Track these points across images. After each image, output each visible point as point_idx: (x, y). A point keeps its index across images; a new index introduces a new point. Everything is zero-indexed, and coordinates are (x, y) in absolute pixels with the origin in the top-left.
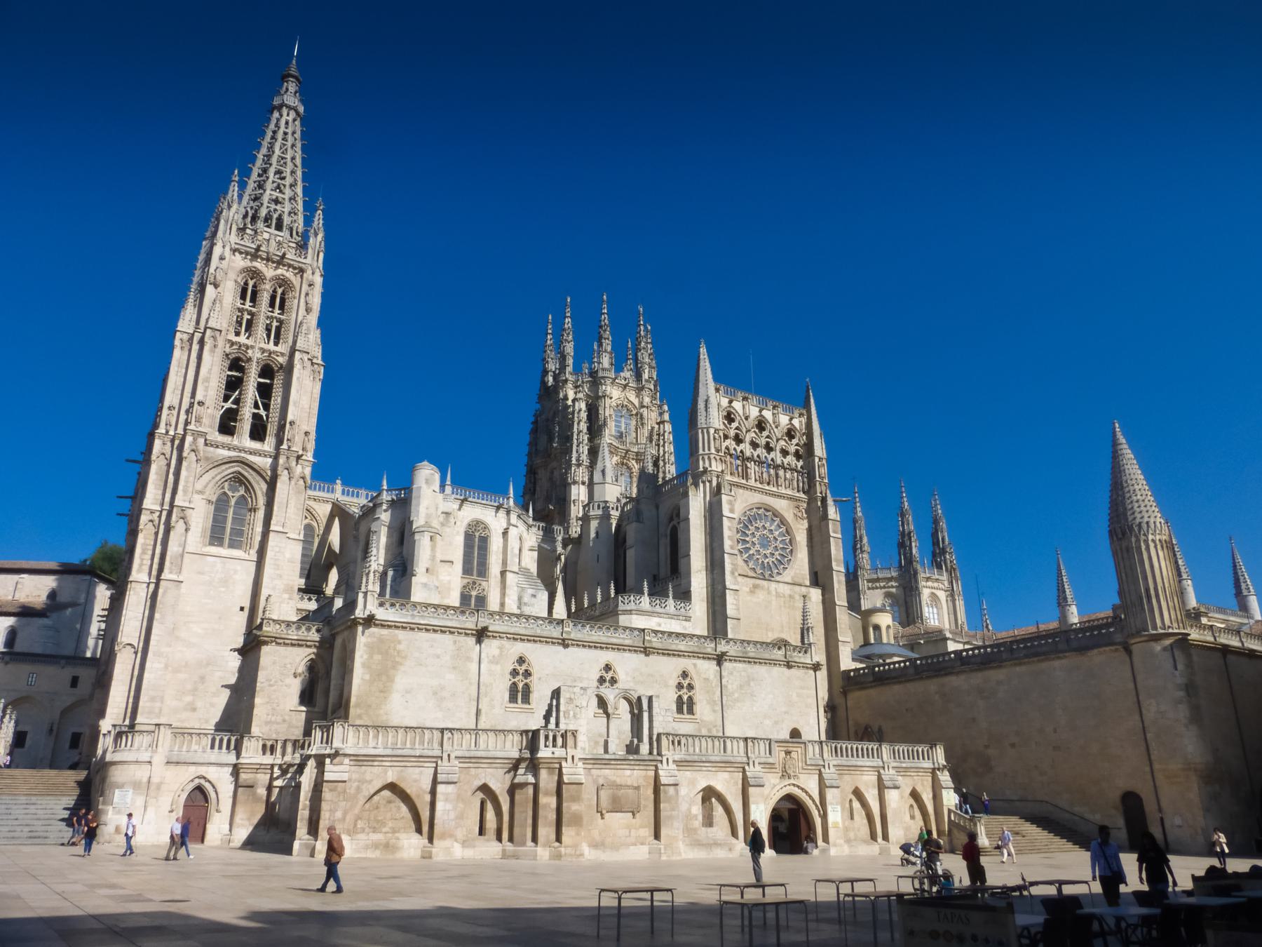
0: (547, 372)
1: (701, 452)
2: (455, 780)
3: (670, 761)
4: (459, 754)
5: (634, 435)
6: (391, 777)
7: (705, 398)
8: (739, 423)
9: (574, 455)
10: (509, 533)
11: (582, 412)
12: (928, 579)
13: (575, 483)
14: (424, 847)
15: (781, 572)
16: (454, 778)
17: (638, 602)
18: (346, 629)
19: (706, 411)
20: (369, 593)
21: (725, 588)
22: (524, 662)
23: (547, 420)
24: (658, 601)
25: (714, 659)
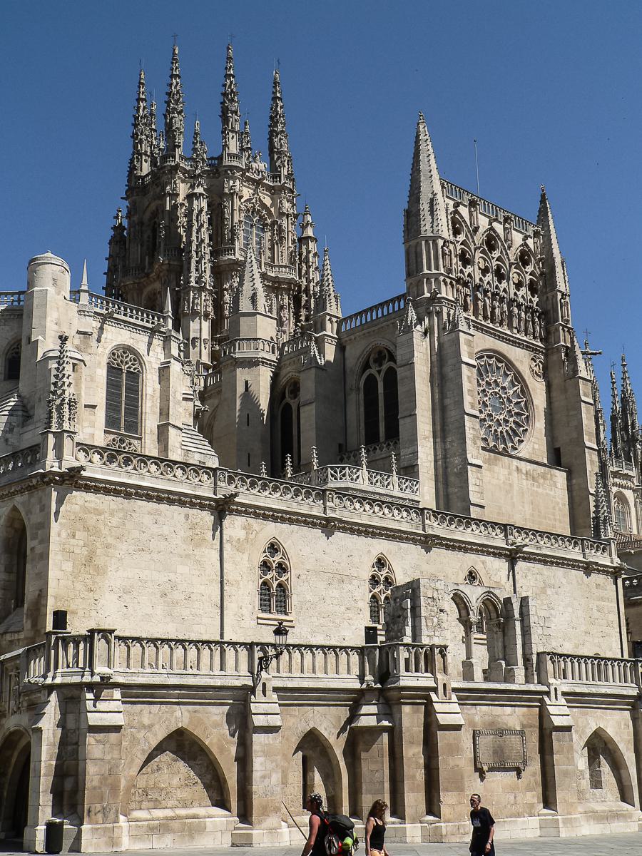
0: (140, 154)
1: (426, 271)
2: (279, 724)
3: (559, 693)
4: (279, 684)
5: (269, 254)
6: (180, 716)
7: (431, 196)
8: (466, 236)
9: (194, 275)
10: (171, 369)
11: (203, 213)
12: (615, 474)
13: (195, 314)
14: (235, 829)
15: (517, 447)
16: (275, 721)
17: (355, 477)
18: (21, 492)
19: (432, 214)
20: (66, 435)
21: (465, 463)
22: (277, 551)
23: (141, 223)
24: (379, 477)
25: (506, 556)
